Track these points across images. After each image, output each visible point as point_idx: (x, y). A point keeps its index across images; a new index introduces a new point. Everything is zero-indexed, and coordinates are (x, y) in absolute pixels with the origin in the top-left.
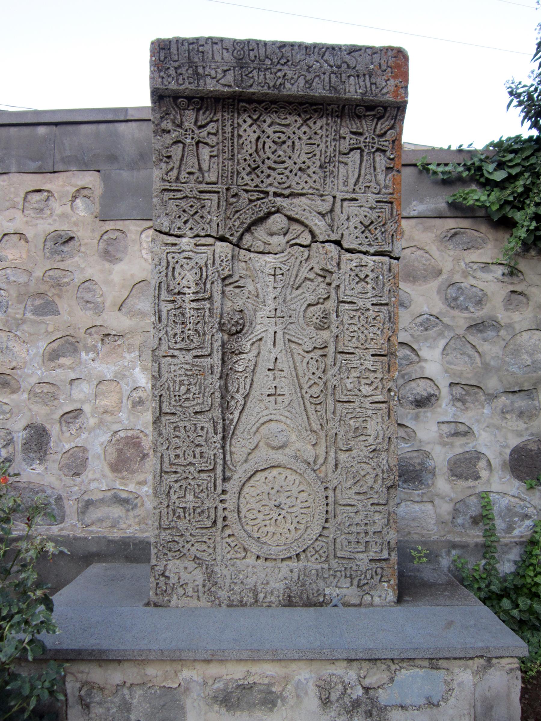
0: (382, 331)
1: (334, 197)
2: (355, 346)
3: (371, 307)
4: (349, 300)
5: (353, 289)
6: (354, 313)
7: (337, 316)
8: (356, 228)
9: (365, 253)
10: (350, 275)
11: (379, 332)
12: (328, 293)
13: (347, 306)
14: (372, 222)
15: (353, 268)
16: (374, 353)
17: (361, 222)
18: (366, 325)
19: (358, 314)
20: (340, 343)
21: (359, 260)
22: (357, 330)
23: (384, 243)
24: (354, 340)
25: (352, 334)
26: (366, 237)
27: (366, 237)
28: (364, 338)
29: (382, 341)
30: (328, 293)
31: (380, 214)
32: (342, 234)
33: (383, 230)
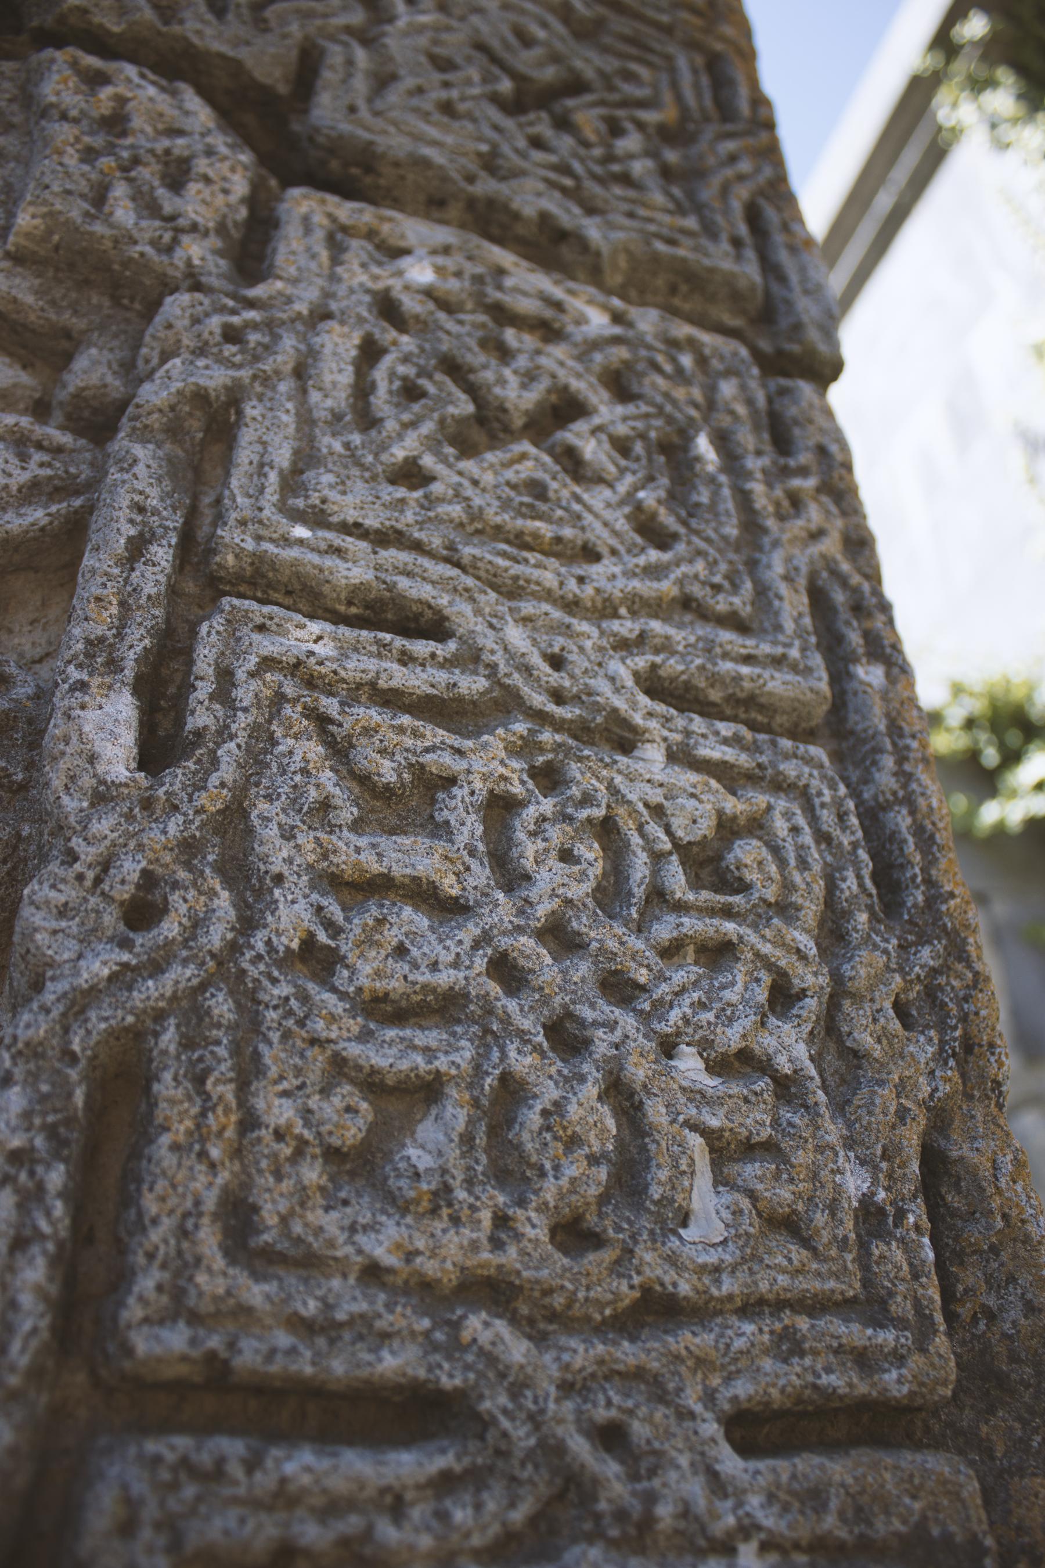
0: (829, 1029)
2: (450, 1250)
3: (640, 709)
4: (355, 569)
5: (411, 474)
6: (435, 744)
7: (160, 744)
10: (370, 352)
11: (790, 1045)
12: (60, 490)
13: (309, 638)
14: (576, 86)
15: (411, 305)
16: (772, 1380)
17: (481, 47)
18: (607, 935)
19: (488, 761)
20: (180, 1184)
22: (475, 977)
24: (430, 1145)
25: (390, 1054)
26: (537, 143)
27: (537, 143)
28: (600, 1125)
29: (855, 1183)
30: (60, 490)
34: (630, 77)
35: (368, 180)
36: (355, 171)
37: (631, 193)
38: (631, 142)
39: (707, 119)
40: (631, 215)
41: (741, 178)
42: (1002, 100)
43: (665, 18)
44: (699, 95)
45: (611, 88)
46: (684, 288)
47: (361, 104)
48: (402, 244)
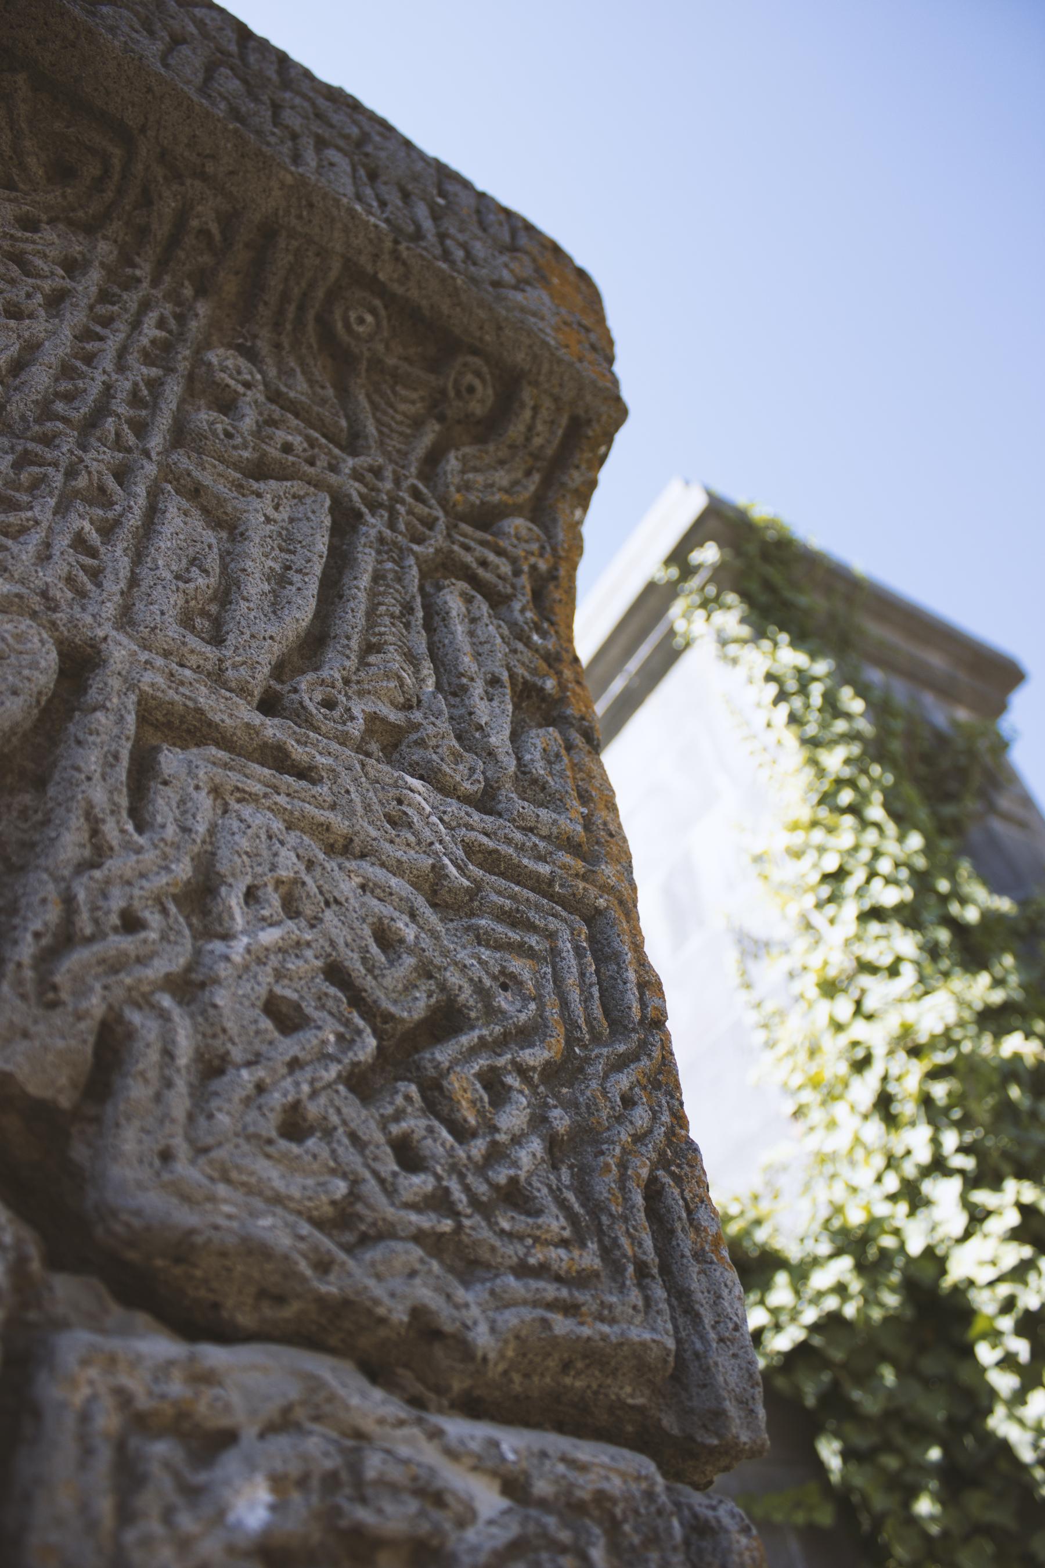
1: (79, 664)
8: (286, 1017)
9: (415, 1361)
21: (317, 1447)
23: (589, 1258)
26: (408, 1154)
31: (518, 965)
32: (111, 1046)
33: (561, 1120)
34: (508, 981)
35: (178, 1271)
36: (159, 1263)
37: (522, 1223)
38: (513, 1118)
39: (596, 1038)
40: (522, 1270)
41: (639, 1138)
42: (730, 619)
43: (544, 869)
44: (587, 1000)
45: (491, 1012)
46: (580, 1365)
47: (181, 1148)
48: (224, 1422)
